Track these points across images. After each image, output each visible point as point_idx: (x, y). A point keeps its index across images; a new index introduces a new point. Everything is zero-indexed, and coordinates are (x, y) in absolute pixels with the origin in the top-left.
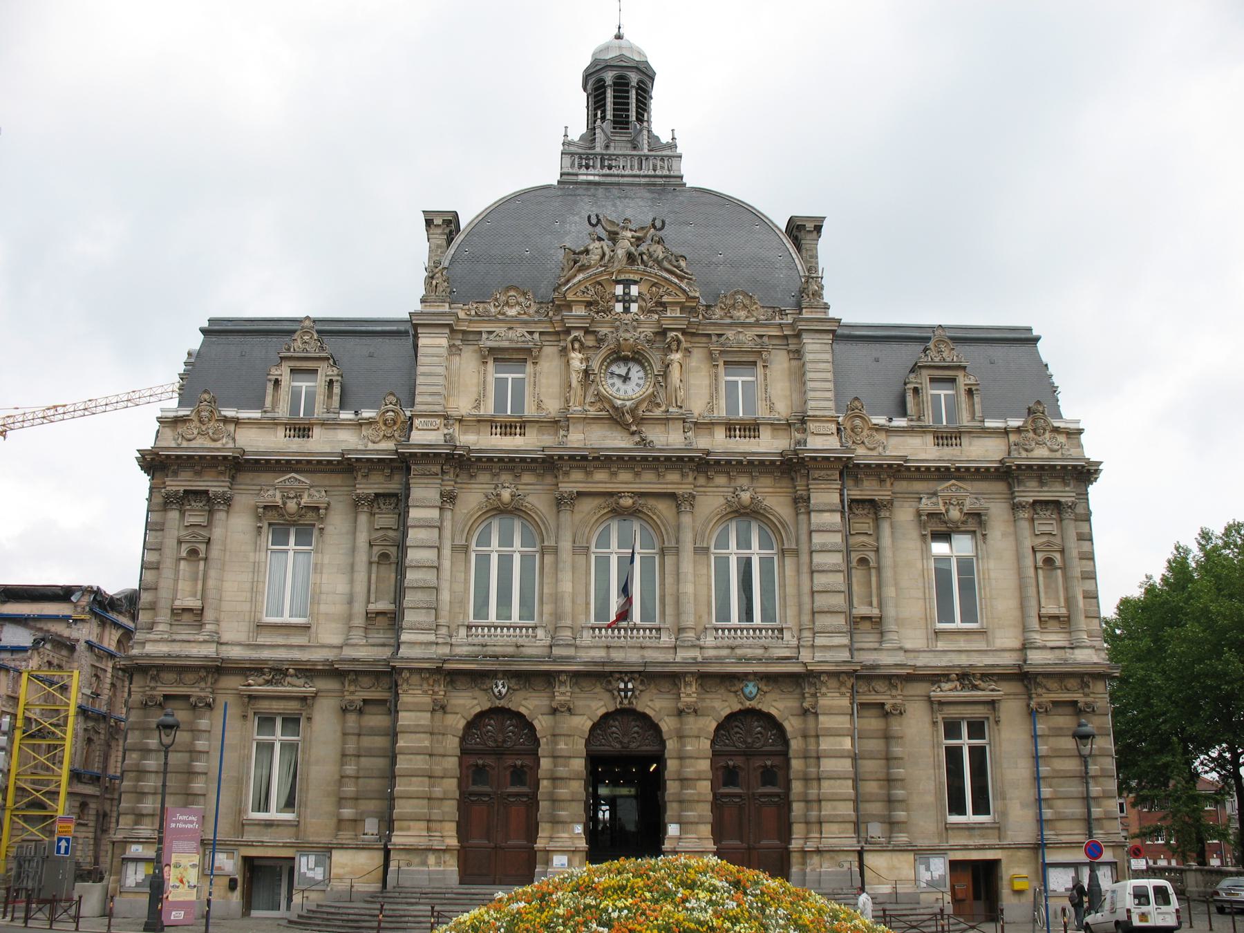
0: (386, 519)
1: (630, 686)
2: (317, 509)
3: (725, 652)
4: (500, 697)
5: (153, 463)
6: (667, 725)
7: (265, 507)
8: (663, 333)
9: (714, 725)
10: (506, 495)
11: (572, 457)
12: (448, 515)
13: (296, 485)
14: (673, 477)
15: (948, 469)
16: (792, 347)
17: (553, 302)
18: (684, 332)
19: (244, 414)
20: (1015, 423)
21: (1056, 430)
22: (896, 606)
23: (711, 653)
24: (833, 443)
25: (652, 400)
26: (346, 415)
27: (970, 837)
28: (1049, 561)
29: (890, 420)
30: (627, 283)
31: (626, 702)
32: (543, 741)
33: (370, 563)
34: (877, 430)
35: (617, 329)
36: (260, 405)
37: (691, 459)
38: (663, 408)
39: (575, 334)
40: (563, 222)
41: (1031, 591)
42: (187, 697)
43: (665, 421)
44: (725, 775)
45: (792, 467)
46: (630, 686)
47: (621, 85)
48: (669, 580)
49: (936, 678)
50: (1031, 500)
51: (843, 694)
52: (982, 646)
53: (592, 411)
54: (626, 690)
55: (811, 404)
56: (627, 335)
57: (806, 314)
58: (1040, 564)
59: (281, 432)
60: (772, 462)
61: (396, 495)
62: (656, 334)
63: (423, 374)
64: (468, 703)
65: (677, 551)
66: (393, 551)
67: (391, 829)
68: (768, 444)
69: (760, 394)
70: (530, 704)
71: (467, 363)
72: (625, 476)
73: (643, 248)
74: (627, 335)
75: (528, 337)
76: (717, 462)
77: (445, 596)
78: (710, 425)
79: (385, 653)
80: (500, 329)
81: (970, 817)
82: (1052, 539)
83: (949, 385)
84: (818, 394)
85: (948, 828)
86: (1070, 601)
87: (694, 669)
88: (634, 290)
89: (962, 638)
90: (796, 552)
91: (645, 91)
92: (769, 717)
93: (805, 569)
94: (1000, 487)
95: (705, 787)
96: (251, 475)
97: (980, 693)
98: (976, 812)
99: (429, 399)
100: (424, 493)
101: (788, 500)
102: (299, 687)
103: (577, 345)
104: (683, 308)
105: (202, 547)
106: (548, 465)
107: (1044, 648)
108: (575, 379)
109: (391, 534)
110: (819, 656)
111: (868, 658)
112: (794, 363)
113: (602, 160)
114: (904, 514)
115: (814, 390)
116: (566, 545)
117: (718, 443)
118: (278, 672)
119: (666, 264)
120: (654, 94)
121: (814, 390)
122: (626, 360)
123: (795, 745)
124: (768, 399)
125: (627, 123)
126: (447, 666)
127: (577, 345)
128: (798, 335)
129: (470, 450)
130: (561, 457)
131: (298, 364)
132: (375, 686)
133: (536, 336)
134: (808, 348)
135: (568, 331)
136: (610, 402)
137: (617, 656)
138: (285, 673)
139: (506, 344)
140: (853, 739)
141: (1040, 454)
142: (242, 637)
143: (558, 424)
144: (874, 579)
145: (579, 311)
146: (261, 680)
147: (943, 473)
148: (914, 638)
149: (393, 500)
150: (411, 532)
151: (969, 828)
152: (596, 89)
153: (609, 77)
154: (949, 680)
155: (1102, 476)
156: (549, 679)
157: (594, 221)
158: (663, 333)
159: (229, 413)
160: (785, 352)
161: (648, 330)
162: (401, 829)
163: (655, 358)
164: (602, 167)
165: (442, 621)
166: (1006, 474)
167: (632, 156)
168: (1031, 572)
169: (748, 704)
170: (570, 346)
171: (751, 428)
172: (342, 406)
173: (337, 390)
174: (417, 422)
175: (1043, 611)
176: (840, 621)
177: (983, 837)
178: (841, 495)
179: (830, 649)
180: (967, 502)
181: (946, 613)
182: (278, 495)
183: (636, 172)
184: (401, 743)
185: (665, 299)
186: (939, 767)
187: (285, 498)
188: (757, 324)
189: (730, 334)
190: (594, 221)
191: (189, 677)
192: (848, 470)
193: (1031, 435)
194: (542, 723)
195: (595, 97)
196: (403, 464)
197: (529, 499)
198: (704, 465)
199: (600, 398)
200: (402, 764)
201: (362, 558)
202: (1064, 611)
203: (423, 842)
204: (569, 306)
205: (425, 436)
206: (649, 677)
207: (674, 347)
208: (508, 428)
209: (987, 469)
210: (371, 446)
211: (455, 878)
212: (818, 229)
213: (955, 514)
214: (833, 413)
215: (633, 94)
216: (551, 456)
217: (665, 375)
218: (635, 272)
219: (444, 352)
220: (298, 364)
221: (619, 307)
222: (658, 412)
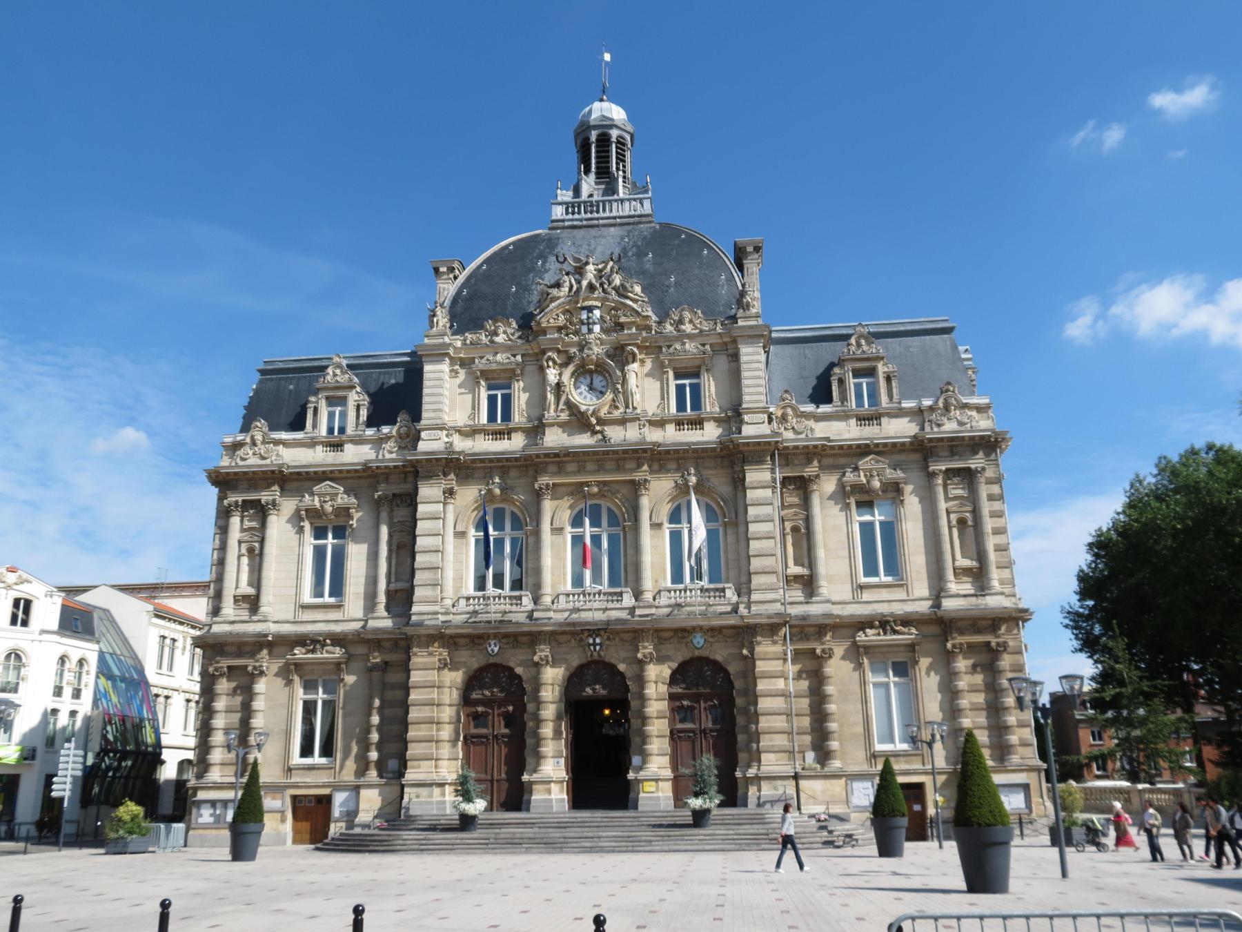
0: (401, 513)
1: (598, 641)
12: (450, 508)
15: (867, 445)
16: (730, 352)
18: (638, 347)
24: (765, 429)
31: (595, 654)
38: (622, 410)
46: (598, 641)
48: (630, 552)
49: (863, 624)
50: (944, 468)
52: (903, 596)
54: (595, 644)
58: (954, 522)
63: (428, 395)
89: (884, 591)
94: (916, 457)
97: (900, 637)
100: (429, 492)
107: (958, 596)
112: (733, 364)
115: (749, 386)
121: (749, 386)
127: (551, 363)
128: (735, 341)
147: (864, 450)
150: (419, 523)
153: (594, 135)
154: (871, 628)
157: (561, 259)
160: (724, 357)
162: (413, 767)
168: (945, 530)
171: (698, 423)
177: (907, 762)
181: (871, 570)
185: (623, 319)
190: (561, 259)
205: (430, 444)
207: (630, 359)
208: (498, 434)
216: (530, 456)
218: (596, 299)
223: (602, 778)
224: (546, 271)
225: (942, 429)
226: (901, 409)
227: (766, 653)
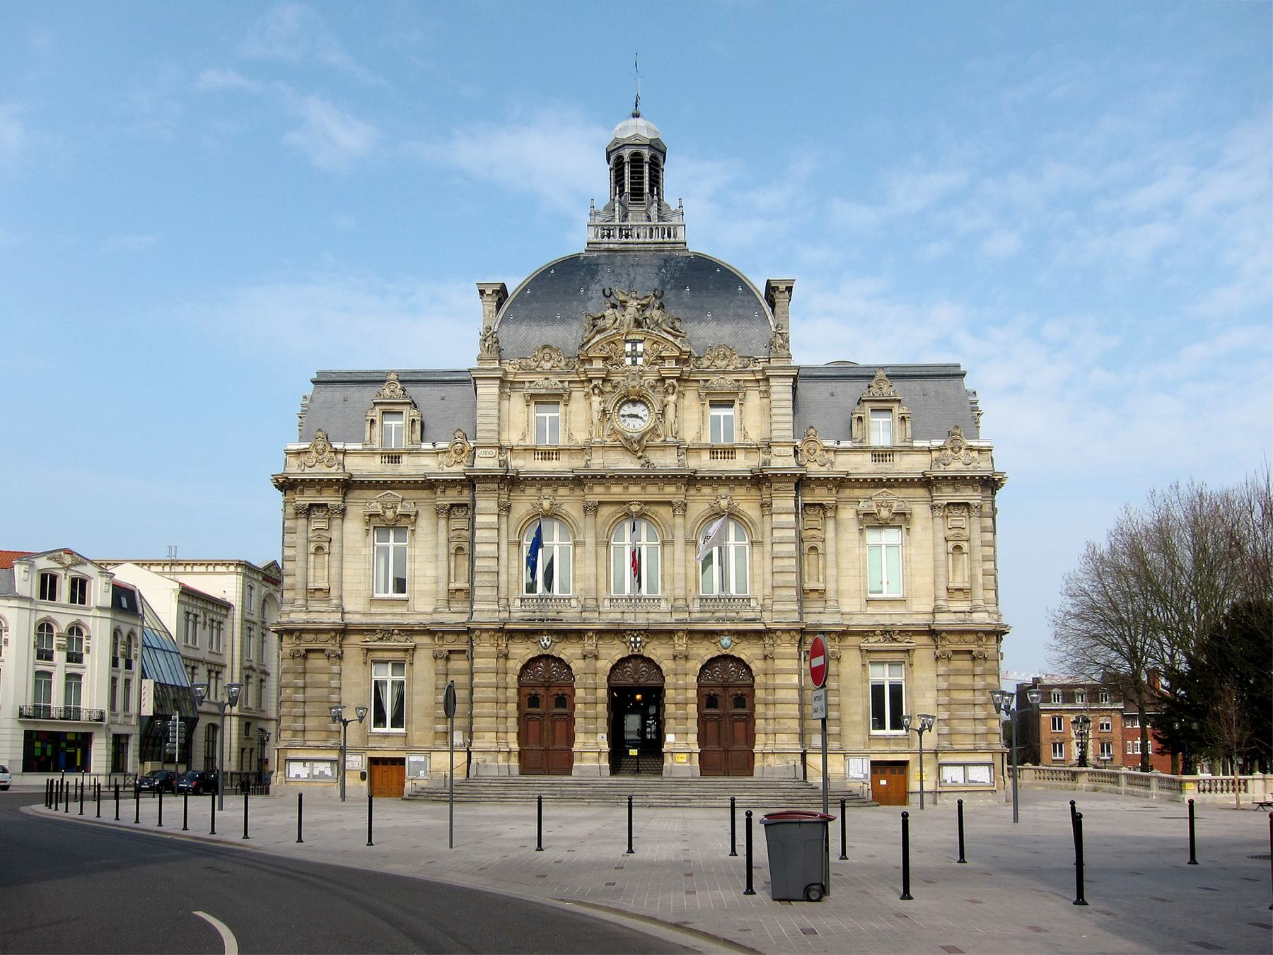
2: (409, 516)
3: (708, 615)
4: (546, 647)
5: (287, 485)
6: (666, 666)
7: (370, 515)
8: (663, 380)
9: (700, 666)
10: (546, 504)
11: (594, 477)
12: (504, 519)
13: (392, 499)
14: (670, 489)
15: (881, 480)
16: (763, 388)
18: (678, 379)
20: (937, 443)
21: (971, 449)
22: (837, 581)
23: (698, 615)
24: (791, 463)
25: (653, 431)
26: (427, 446)
27: (887, 744)
28: (958, 548)
29: (838, 443)
30: (634, 342)
32: (577, 678)
33: (449, 554)
34: (827, 451)
35: (627, 377)
36: (362, 440)
37: (683, 476)
39: (595, 382)
40: (587, 289)
41: (942, 571)
42: (323, 651)
43: (663, 447)
44: (708, 701)
45: (759, 480)
47: (637, 160)
48: (667, 564)
49: (864, 634)
51: (793, 645)
52: (902, 610)
53: (609, 442)
54: (636, 642)
55: (775, 433)
56: (634, 383)
57: (774, 363)
59: (378, 459)
60: (744, 478)
61: (466, 505)
62: (657, 381)
63: (482, 416)
64: (522, 651)
65: (672, 543)
66: (466, 546)
67: (471, 738)
68: (742, 464)
69: (736, 425)
70: (569, 652)
71: (516, 405)
72: (634, 489)
73: (647, 313)
74: (634, 383)
75: (560, 385)
76: (703, 478)
77: (503, 577)
78: (699, 449)
79: (464, 618)
80: (539, 379)
81: (888, 731)
82: (961, 531)
83: (887, 414)
84: (780, 426)
85: (871, 738)
86: (972, 577)
87: (684, 627)
88: (640, 347)
89: (886, 605)
90: (761, 543)
91: (658, 165)
92: (739, 660)
93: (768, 556)
94: (921, 492)
95: (692, 709)
96: (358, 492)
98: (892, 728)
99: (488, 435)
100: (486, 505)
101: (757, 505)
102: (401, 642)
103: (596, 391)
104: (678, 360)
105: (326, 545)
106: (578, 482)
108: (596, 416)
109: (464, 533)
110: (776, 617)
111: (810, 619)
112: (764, 400)
113: (621, 230)
114: (847, 514)
116: (590, 540)
117: (703, 463)
118: (387, 632)
119: (664, 326)
120: (665, 167)
122: (634, 402)
123: (759, 680)
124: (743, 429)
125: (642, 195)
126: (507, 627)
127: (596, 391)
128: (767, 379)
129: (518, 473)
130: (586, 477)
131: (387, 408)
132: (456, 640)
133: (566, 384)
134: (773, 389)
135: (590, 380)
136: (622, 434)
137: (629, 618)
138: (391, 633)
139: (544, 391)
140: (800, 675)
141: (956, 467)
142: (360, 608)
145: (598, 364)
146: (375, 638)
147: (878, 483)
148: (850, 604)
149: (464, 509)
150: (478, 533)
151: (887, 739)
152: (616, 165)
153: (626, 154)
155: (1006, 482)
156: (580, 634)
157: (607, 293)
158: (663, 380)
161: (651, 378)
163: (656, 399)
164: (621, 237)
165: (502, 595)
166: (927, 483)
169: (724, 652)
171: (729, 452)
173: (418, 427)
174: (478, 452)
175: (951, 585)
176: (793, 592)
177: (896, 745)
178: (796, 501)
179: (784, 613)
182: (380, 507)
183: (648, 240)
184: (476, 680)
186: (867, 696)
188: (737, 371)
189: (714, 379)
191: (324, 637)
192: (802, 483)
193: (949, 452)
194: (577, 665)
196: (470, 482)
197: (564, 507)
198: (692, 480)
199: (614, 431)
200: (477, 694)
201: (443, 551)
202: (967, 585)
203: (494, 746)
204: (590, 360)
205: (486, 462)
206: (652, 633)
208: (547, 454)
209: (912, 480)
210: (447, 470)
211: (516, 771)
212: (789, 289)
213: (884, 513)
214: (791, 439)
217: (663, 414)
219: (496, 398)
220: (387, 408)
221: (628, 361)
222: (658, 441)
223: (636, 750)
227: (784, 654)
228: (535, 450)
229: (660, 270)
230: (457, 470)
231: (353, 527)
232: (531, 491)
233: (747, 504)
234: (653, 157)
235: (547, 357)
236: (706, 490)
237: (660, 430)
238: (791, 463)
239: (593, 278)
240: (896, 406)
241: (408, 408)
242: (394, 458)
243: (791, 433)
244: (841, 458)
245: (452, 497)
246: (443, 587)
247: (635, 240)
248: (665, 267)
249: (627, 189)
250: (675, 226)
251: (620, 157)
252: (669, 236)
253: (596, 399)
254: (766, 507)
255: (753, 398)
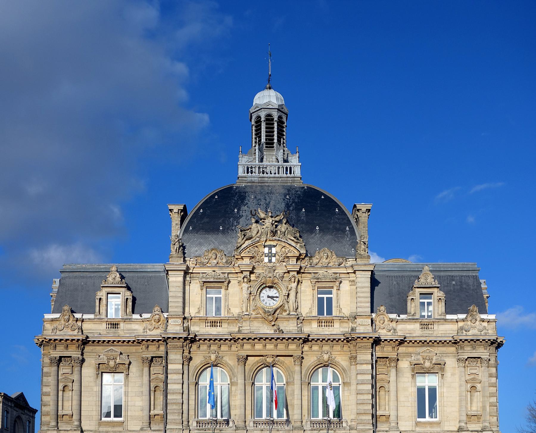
7: (99, 364)
10: (213, 357)
16: (351, 279)
17: (234, 256)
19: (86, 316)
26: (136, 316)
36: (93, 312)
38: (288, 312)
40: (239, 210)
43: (288, 319)
47: (269, 119)
59: (104, 325)
61: (162, 357)
68: (338, 329)
72: (270, 346)
84: (362, 304)
93: (354, 392)
94: (453, 349)
99: (176, 310)
101: (347, 358)
113: (259, 168)
124: (339, 306)
125: (273, 143)
129: (196, 336)
139: (212, 280)
143: (238, 319)
144: (387, 397)
145: (247, 261)
147: (423, 343)
152: (256, 122)
153: (263, 114)
159: (78, 316)
160: (348, 281)
164: (259, 173)
167: (275, 166)
170: (242, 280)
171: (329, 323)
172: (133, 312)
173: (130, 304)
178: (372, 355)
180: (434, 358)
182: (105, 358)
183: (277, 175)
187: (109, 359)
195: (256, 127)
197: (224, 358)
210: (149, 333)
215: (276, 125)
224: (241, 217)
225: (470, 333)
226: (446, 319)
228: (205, 320)
229: (285, 196)
230: (156, 333)
231: (88, 371)
232: (204, 347)
233: (341, 357)
234: (280, 117)
235: (214, 257)
236: (315, 348)
237: (286, 307)
238: (369, 328)
239: (242, 202)
240: (435, 290)
241: (124, 289)
242: (114, 325)
243: (369, 309)
244: (400, 327)
245: (153, 351)
246: (146, 413)
247: (269, 175)
248: (289, 194)
249: (263, 140)
250: (295, 166)
251: (259, 117)
252: (290, 173)
253: (245, 286)
254: (353, 359)
255: (346, 286)
